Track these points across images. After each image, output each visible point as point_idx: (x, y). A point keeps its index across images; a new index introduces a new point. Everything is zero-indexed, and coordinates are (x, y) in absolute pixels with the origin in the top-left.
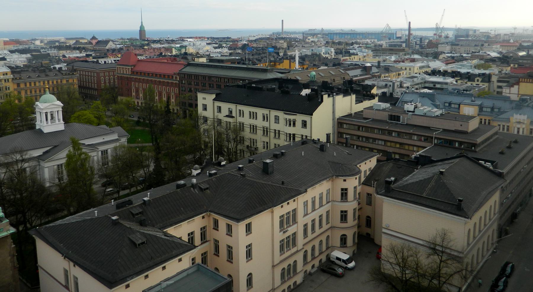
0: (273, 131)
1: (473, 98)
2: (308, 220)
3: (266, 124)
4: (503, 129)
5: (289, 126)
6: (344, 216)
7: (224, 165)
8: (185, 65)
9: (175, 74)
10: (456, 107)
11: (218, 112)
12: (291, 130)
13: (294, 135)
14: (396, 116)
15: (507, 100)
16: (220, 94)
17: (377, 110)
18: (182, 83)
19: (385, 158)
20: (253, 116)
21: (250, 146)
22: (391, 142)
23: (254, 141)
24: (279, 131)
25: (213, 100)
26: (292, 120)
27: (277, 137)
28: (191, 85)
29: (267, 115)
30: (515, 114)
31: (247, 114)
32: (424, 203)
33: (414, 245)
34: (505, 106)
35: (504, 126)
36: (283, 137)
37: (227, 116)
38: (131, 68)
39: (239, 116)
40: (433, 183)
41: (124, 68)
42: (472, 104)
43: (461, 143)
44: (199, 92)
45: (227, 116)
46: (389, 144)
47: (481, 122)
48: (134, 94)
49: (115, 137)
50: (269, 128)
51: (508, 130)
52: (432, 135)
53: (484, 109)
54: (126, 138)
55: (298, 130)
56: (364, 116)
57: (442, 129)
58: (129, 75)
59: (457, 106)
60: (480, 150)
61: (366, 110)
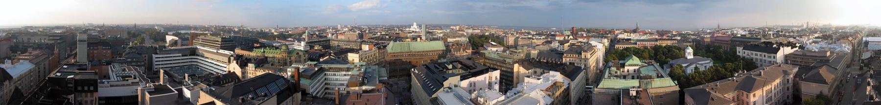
3: (761, 58)
12: (770, 60)
20: (756, 55)
31: (754, 54)
49: (709, 61)
55: (772, 59)
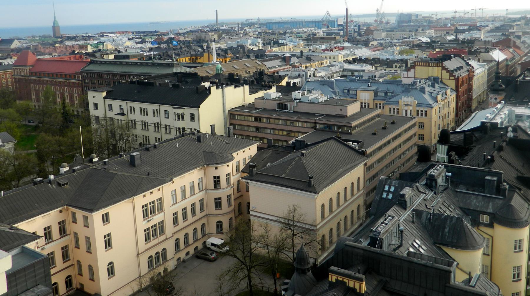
0: (164, 126)
1: (369, 84)
2: (178, 208)
3: (157, 120)
4: (394, 111)
5: (178, 120)
6: (218, 203)
7: (96, 162)
8: (88, 63)
9: (76, 73)
10: (354, 93)
11: (109, 111)
12: (181, 124)
13: (183, 129)
14: (281, 105)
15: (400, 84)
16: (111, 91)
17: (267, 99)
18: (85, 83)
19: (266, 146)
20: (144, 112)
21: (143, 143)
22: (278, 130)
23: (147, 138)
24: (169, 126)
25: (104, 98)
26: (180, 114)
27: (168, 132)
28: (95, 84)
29: (157, 110)
30: (403, 97)
31: (138, 111)
32: (282, 183)
33: (265, 221)
34: (399, 89)
35: (394, 109)
36: (173, 132)
37: (119, 114)
38: (30, 69)
39: (131, 114)
40: (293, 165)
41: (21, 69)
42: (368, 90)
43: (339, 127)
44: (89, 90)
45: (119, 114)
46: (277, 132)
47: (362, 106)
48: (34, 97)
50: (159, 124)
51: (398, 112)
52: (313, 121)
53: (379, 94)
54: (13, 144)
55: (187, 124)
56: (256, 107)
57: (325, 114)
58: (27, 76)
59: (354, 92)
60: (357, 133)
61: (257, 100)
